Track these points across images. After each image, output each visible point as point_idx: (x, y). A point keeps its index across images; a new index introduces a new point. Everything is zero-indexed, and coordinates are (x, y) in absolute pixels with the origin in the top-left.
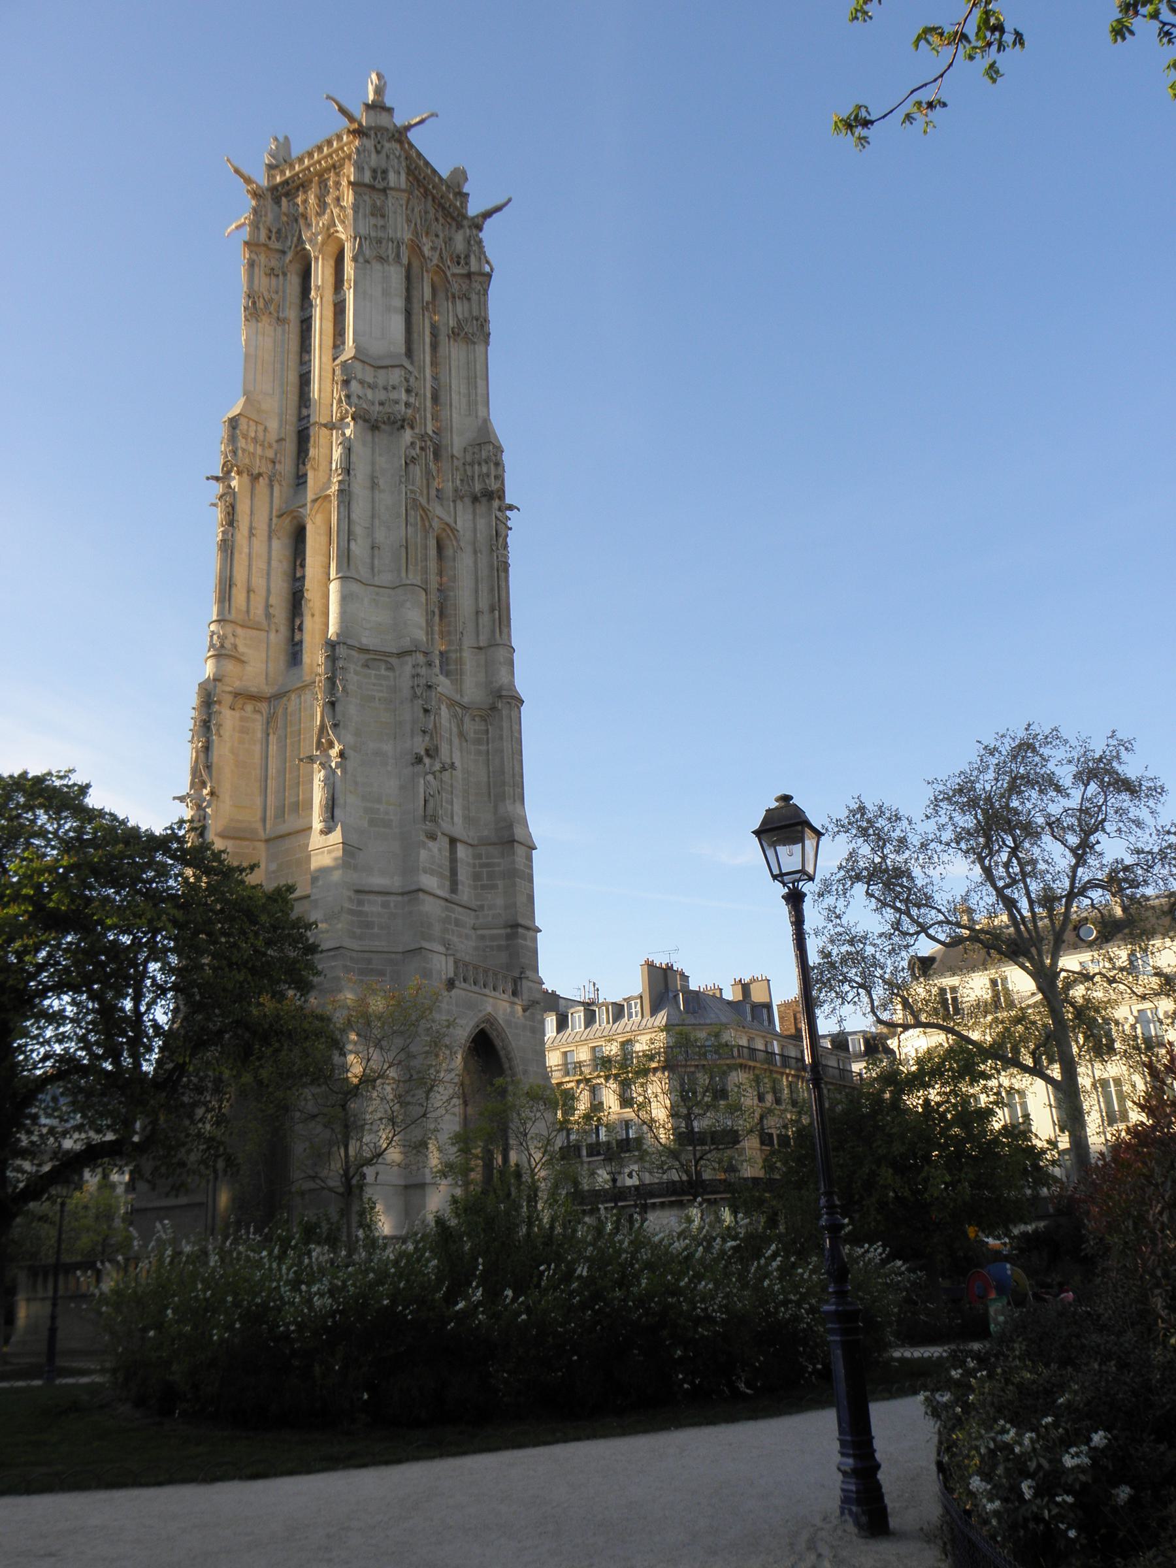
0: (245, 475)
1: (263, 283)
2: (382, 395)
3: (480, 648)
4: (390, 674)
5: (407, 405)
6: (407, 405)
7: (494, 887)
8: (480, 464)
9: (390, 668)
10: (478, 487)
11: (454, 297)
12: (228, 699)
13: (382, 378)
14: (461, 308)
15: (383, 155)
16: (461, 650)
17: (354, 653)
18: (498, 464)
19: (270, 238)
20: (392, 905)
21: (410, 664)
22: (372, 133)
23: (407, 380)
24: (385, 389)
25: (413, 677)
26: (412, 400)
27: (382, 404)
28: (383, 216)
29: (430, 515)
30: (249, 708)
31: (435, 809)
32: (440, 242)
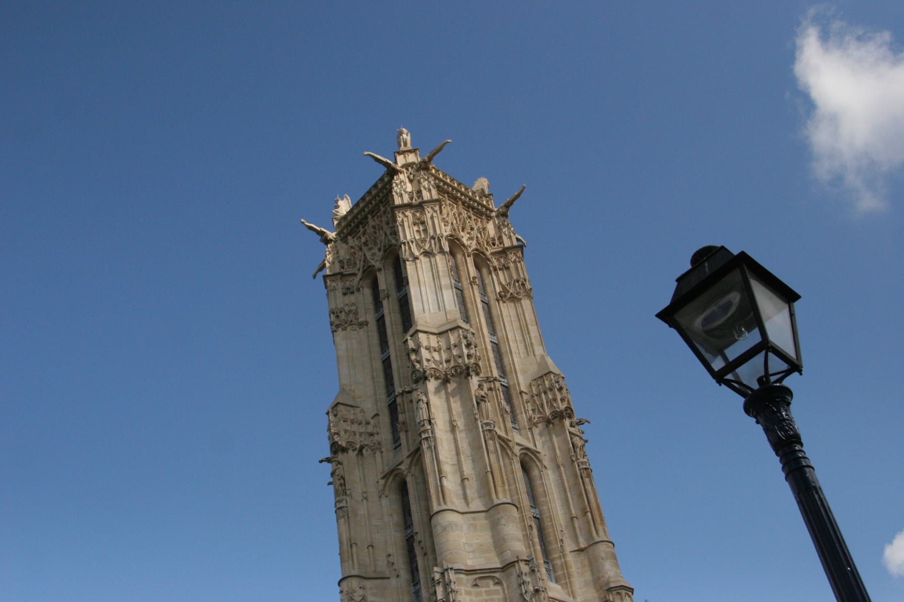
0: (350, 452)
1: (340, 301)
3: (581, 550)
11: (495, 269)
16: (564, 556)
17: (462, 576)
19: (343, 268)
26: (472, 351)
29: (511, 444)
32: (475, 233)
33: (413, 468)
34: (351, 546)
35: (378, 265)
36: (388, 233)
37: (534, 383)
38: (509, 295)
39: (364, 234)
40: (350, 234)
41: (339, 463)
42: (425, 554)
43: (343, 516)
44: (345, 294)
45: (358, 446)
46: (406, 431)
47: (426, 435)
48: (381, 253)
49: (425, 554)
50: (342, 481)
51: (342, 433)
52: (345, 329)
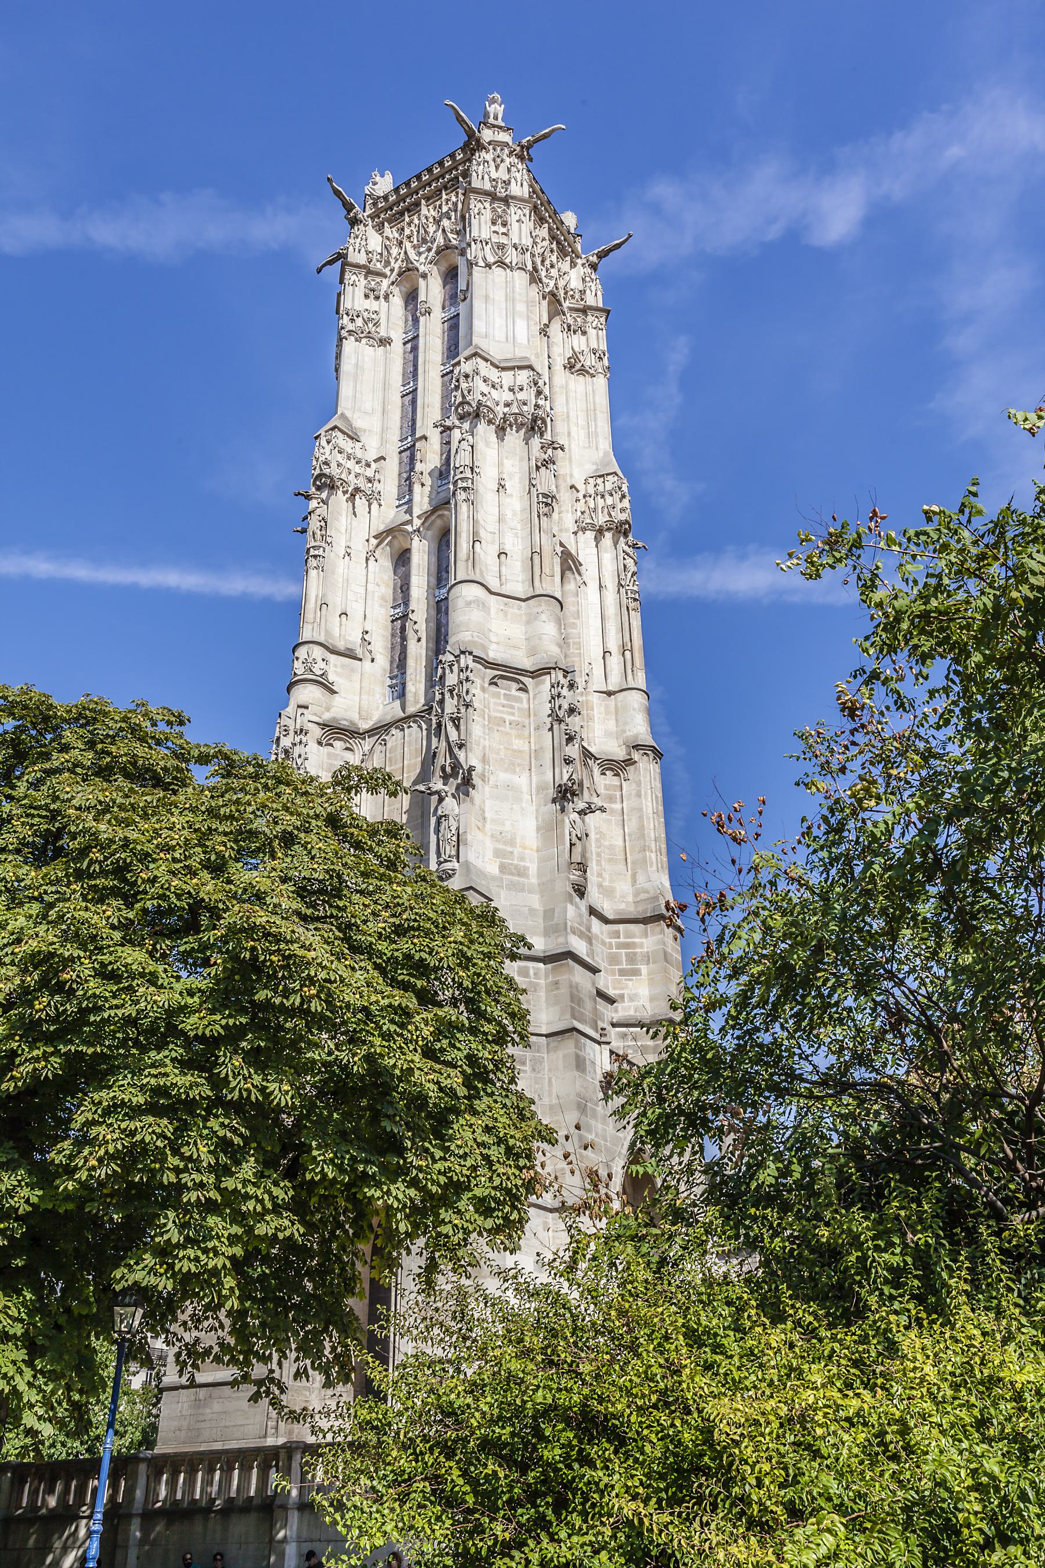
2: (508, 396)
3: (609, 694)
5: (537, 406)
6: (537, 406)
7: (636, 973)
8: (603, 496)
10: (602, 519)
12: (316, 732)
13: (507, 378)
14: (578, 342)
15: (503, 167)
20: (531, 972)
21: (548, 685)
23: (536, 384)
24: (511, 390)
26: (541, 402)
28: (504, 225)
31: (583, 856)
37: (591, 481)
38: (578, 366)
39: (409, 224)
44: (367, 296)
47: (465, 485)
49: (419, 640)
51: (334, 465)
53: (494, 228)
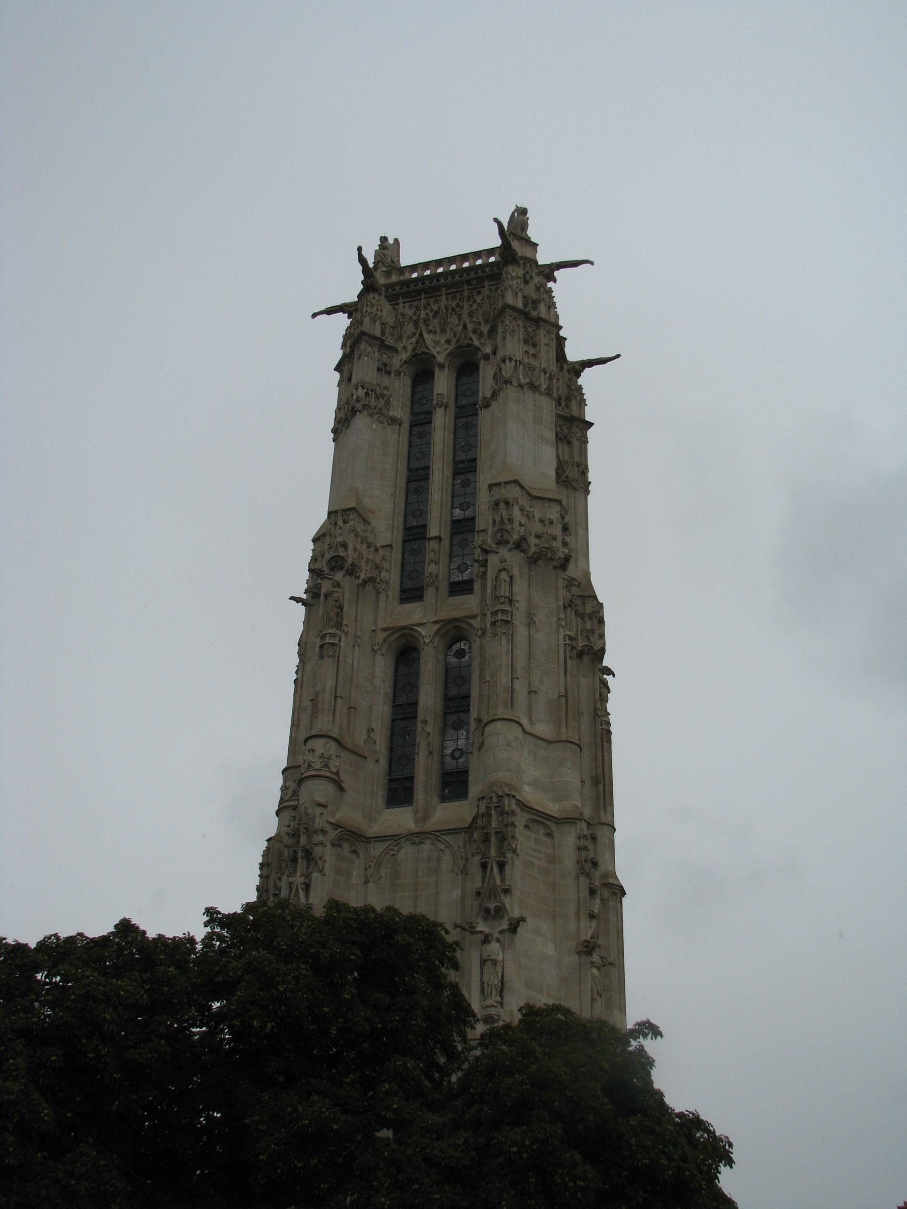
2: (538, 528)
4: (548, 840)
9: (550, 835)
18: (601, 622)
22: (522, 262)
24: (542, 521)
25: (579, 849)
27: (538, 536)
28: (534, 345)
30: (346, 846)
33: (437, 639)
34: (335, 698)
35: (440, 359)
36: (470, 327)
39: (426, 307)
40: (405, 295)
41: (338, 585)
42: (431, 753)
43: (333, 657)
44: (379, 370)
45: (362, 576)
46: (437, 589)
48: (451, 348)
49: (431, 753)
50: (339, 610)
52: (371, 415)
53: (526, 348)
